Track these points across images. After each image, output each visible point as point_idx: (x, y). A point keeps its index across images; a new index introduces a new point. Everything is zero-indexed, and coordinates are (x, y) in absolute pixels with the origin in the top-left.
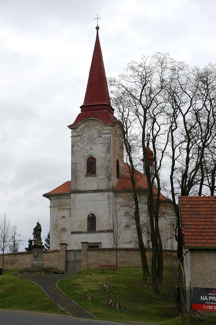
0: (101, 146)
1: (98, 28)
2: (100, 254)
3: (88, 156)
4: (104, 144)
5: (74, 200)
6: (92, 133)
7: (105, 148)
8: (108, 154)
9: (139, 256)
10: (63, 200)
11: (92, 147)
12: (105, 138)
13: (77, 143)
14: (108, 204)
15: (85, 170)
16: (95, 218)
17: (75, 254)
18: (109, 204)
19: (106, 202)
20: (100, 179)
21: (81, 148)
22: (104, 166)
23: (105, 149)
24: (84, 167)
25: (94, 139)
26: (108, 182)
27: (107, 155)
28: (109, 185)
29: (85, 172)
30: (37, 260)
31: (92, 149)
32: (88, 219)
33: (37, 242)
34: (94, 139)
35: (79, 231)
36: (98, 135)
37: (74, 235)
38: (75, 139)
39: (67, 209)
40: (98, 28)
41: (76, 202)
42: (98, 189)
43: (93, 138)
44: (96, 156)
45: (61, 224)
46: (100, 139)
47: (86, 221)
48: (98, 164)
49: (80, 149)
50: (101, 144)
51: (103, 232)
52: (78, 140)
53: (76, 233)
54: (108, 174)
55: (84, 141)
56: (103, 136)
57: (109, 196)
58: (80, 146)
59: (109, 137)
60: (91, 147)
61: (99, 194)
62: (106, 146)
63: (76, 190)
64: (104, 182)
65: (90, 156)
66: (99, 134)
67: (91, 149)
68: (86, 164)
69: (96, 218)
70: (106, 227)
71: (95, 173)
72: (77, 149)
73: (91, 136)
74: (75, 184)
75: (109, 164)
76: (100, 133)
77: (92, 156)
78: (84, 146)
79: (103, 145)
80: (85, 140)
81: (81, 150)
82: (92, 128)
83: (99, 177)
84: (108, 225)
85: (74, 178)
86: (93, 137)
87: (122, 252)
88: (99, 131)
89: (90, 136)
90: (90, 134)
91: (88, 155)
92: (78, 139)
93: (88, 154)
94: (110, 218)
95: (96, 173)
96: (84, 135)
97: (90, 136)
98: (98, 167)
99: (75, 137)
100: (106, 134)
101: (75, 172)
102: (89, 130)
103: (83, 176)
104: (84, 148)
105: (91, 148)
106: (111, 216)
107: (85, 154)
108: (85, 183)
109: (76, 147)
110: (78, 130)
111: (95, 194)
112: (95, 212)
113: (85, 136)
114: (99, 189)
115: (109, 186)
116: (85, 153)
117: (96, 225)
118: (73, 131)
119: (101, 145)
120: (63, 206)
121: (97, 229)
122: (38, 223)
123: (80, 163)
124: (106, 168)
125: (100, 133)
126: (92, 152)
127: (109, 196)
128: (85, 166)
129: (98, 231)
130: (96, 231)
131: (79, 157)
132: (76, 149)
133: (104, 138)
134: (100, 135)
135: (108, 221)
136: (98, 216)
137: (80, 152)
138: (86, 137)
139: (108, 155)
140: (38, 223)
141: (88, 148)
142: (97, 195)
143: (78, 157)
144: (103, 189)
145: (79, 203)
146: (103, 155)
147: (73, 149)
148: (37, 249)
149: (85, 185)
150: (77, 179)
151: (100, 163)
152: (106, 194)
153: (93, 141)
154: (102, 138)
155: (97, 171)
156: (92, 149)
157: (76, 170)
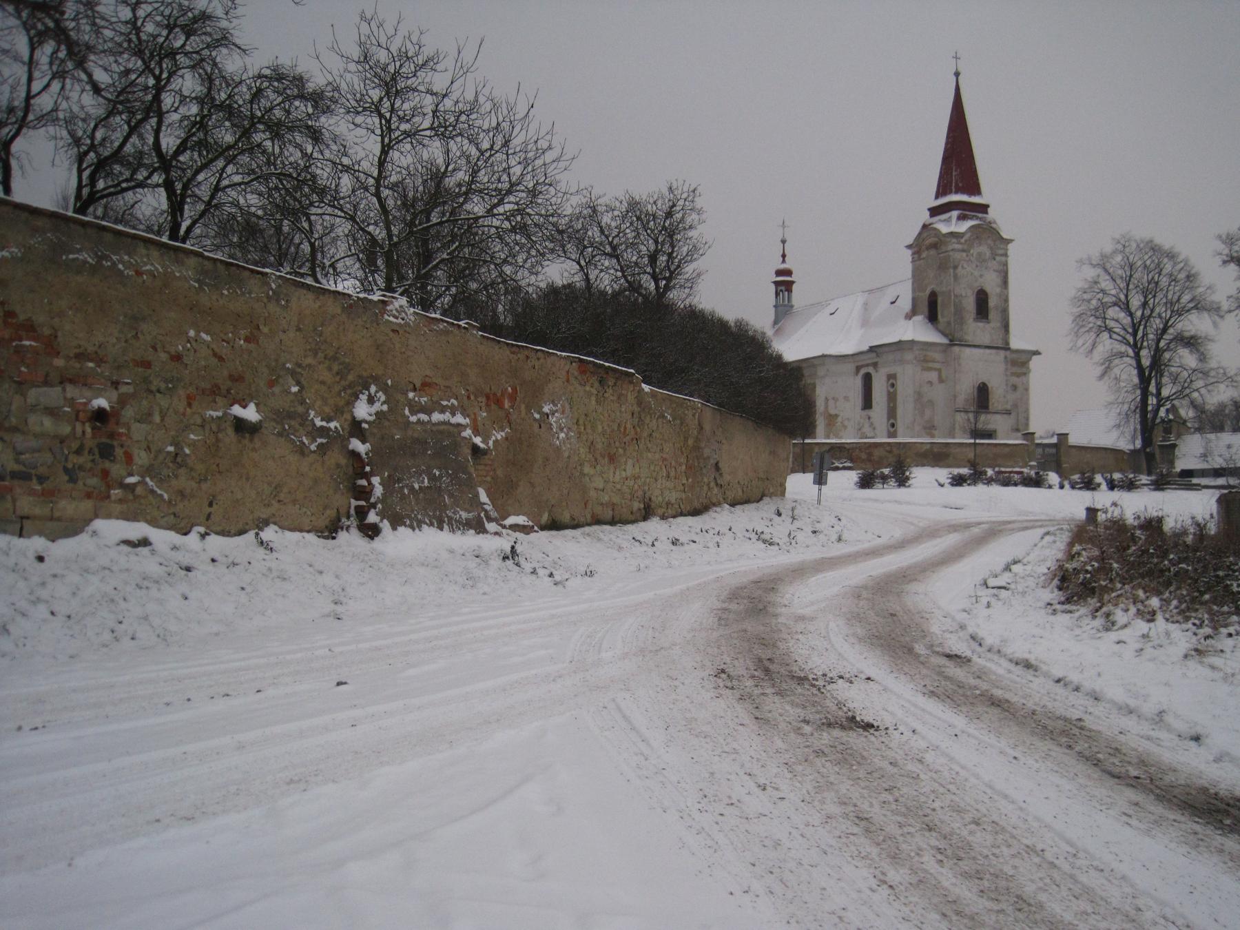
1: (957, 74)
25: (984, 261)
34: (984, 261)
39: (935, 369)
40: (957, 74)
44: (988, 289)
56: (998, 258)
61: (993, 351)
83: (992, 325)
88: (991, 249)
96: (972, 251)
97: (979, 254)
103: (972, 320)
104: (972, 274)
110: (963, 240)
111: (988, 351)
131: (965, 288)
135: (1005, 397)
136: (992, 388)
141: (976, 273)
142: (991, 354)
152: (1002, 353)
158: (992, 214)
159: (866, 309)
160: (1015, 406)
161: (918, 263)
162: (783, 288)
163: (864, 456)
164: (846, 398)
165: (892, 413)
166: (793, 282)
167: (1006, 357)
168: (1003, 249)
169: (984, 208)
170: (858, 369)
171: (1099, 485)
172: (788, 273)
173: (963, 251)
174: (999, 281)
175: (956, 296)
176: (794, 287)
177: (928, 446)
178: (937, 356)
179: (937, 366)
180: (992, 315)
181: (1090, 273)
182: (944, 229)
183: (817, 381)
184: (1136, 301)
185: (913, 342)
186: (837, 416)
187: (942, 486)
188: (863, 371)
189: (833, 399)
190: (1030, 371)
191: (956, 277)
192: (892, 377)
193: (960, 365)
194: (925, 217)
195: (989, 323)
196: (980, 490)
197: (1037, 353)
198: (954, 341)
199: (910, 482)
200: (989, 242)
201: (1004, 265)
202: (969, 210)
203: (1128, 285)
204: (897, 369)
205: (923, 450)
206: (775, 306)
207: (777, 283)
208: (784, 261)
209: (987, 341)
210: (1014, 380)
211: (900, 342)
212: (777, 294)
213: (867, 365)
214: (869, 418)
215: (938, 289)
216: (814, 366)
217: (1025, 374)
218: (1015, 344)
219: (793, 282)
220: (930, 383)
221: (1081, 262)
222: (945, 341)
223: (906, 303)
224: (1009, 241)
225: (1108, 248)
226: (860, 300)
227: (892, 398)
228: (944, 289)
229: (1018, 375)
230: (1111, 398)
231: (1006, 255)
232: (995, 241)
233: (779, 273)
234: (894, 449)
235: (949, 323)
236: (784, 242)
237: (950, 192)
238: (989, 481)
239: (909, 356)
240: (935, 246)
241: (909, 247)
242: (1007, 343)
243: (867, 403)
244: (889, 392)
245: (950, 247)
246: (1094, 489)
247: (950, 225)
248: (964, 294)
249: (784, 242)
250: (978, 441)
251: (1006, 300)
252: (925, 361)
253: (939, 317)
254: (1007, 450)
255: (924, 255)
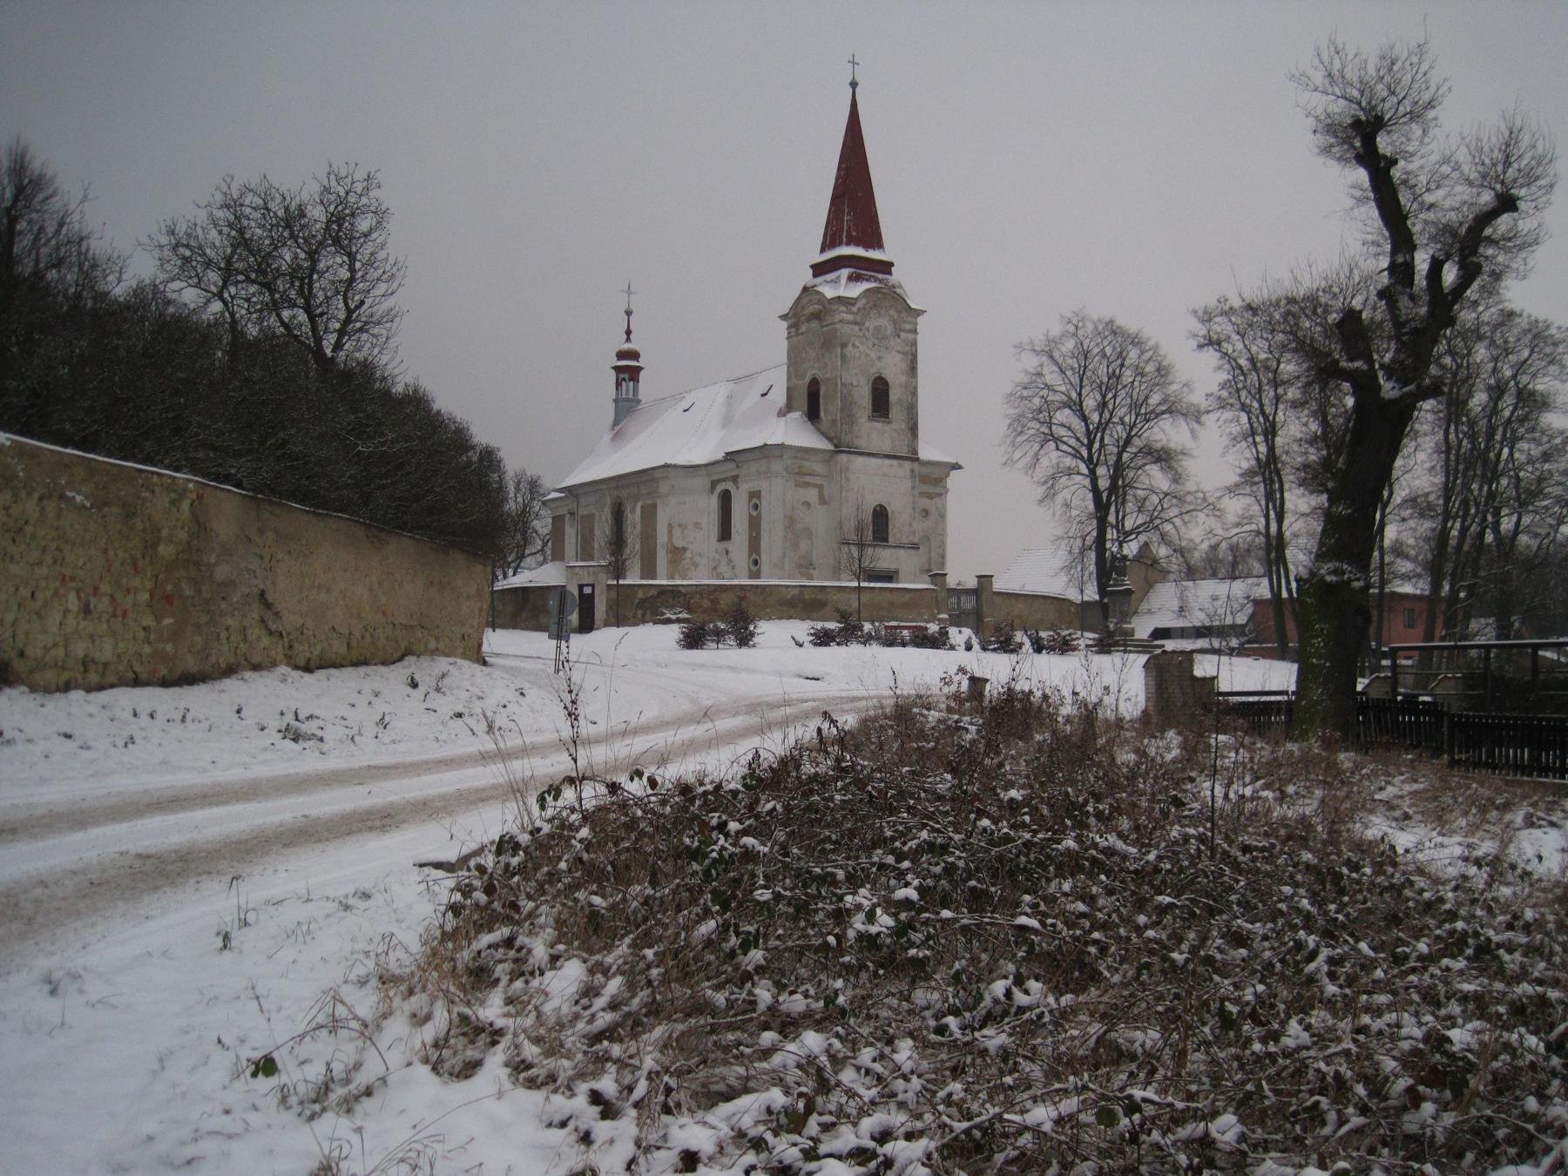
0: (898, 358)
1: (854, 85)
19: (908, 484)
25: (885, 338)
34: (885, 338)
39: (815, 485)
40: (854, 85)
46: (898, 340)
56: (903, 335)
61: (895, 462)
83: (894, 426)
88: (895, 322)
93: (874, 370)
96: (867, 324)
97: (877, 329)
103: (865, 419)
104: (867, 355)
108: (869, 435)
109: (850, 347)
110: (855, 309)
111: (887, 462)
121: (891, 539)
152: (907, 464)
158: (897, 275)
159: (729, 405)
160: (926, 538)
161: (795, 339)
162: (626, 376)
163: (706, 604)
164: (697, 525)
165: (754, 545)
166: (639, 369)
167: (913, 471)
168: (910, 323)
169: (886, 267)
170: (714, 484)
171: (1021, 645)
172: (634, 355)
173: (855, 323)
174: (904, 366)
175: (843, 385)
176: (642, 374)
177: (796, 591)
178: (819, 468)
179: (817, 480)
180: (895, 412)
181: (1031, 362)
182: (829, 292)
183: (658, 501)
184: (1090, 403)
185: (782, 446)
186: (685, 549)
187: (801, 646)
188: (720, 488)
189: (680, 525)
190: (947, 491)
191: (844, 359)
192: (755, 495)
193: (848, 480)
194: (807, 277)
196: (855, 649)
197: (957, 467)
198: (841, 447)
199: (756, 639)
200: (892, 312)
202: (862, 268)
203: (1081, 380)
204: (762, 485)
205: (789, 596)
206: (616, 401)
207: (618, 369)
208: (628, 340)
209: (886, 447)
210: (925, 502)
211: (765, 445)
212: (618, 384)
213: (725, 480)
214: (727, 552)
215: (820, 375)
216: (655, 480)
217: (940, 495)
218: (926, 452)
219: (639, 369)
220: (807, 504)
221: (1020, 348)
222: (830, 447)
223: (779, 396)
224: (919, 313)
225: (1056, 331)
226: (722, 391)
227: (755, 523)
228: (828, 375)
229: (930, 496)
230: (1059, 531)
231: (915, 331)
232: (899, 312)
233: (621, 355)
234: (750, 596)
235: (834, 422)
236: (629, 313)
237: (840, 244)
238: (867, 640)
239: (777, 466)
240: (817, 316)
241: (784, 317)
242: (916, 452)
243: (725, 533)
244: (751, 516)
245: (837, 318)
246: (1012, 651)
247: (838, 287)
248: (855, 383)
249: (629, 313)
250: (863, 584)
251: (914, 393)
252: (800, 473)
253: (822, 414)
254: (908, 597)
255: (803, 329)
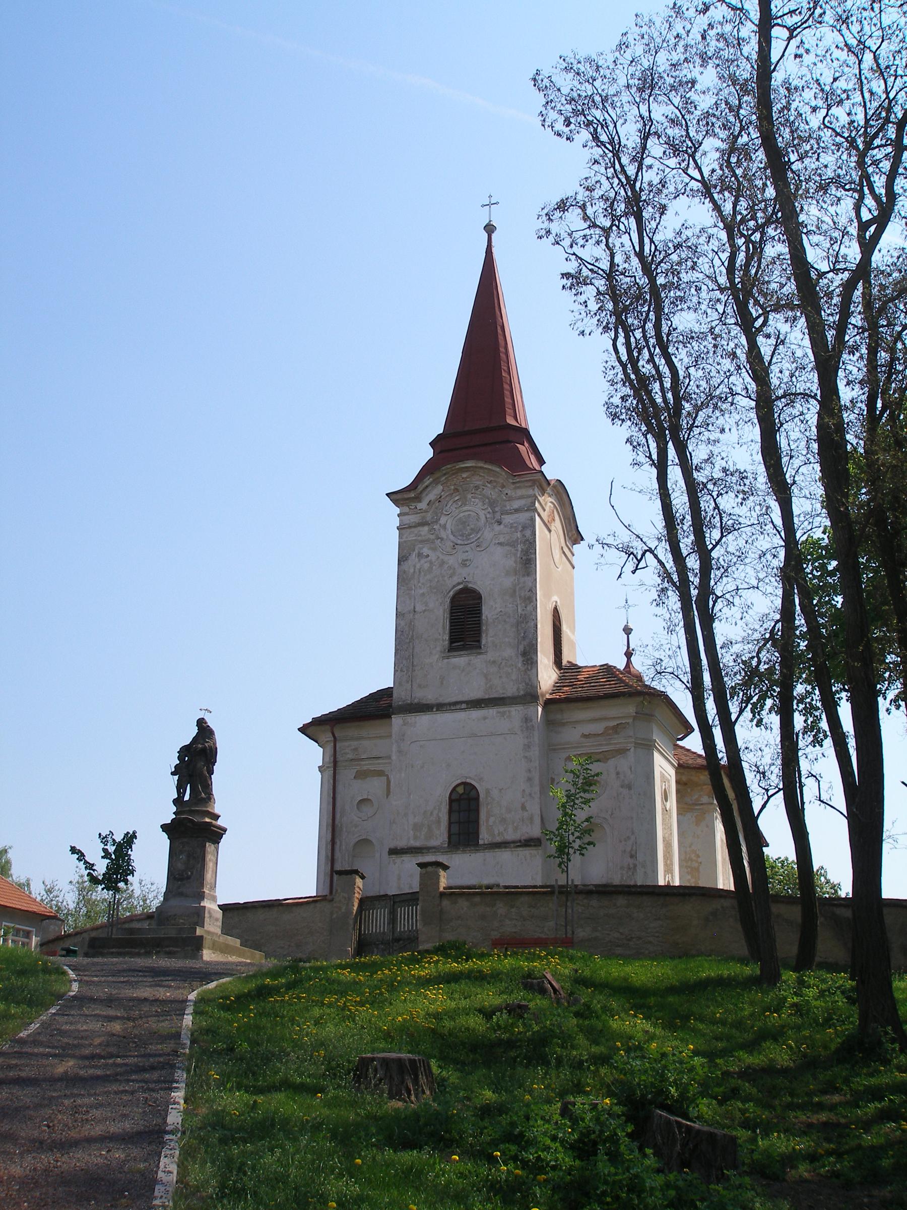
1: (490, 229)
2: (494, 909)
3: (454, 586)
4: (512, 544)
5: (403, 735)
6: (469, 513)
7: (513, 559)
8: (524, 576)
9: (656, 919)
10: (365, 743)
11: (469, 558)
12: (515, 525)
13: (417, 548)
14: (525, 745)
15: (441, 633)
16: (477, 798)
17: (393, 913)
18: (529, 747)
20: (494, 662)
21: (431, 562)
22: (509, 617)
23: (515, 562)
24: (441, 624)
25: (476, 530)
26: (523, 669)
27: (522, 580)
28: (527, 681)
29: (443, 640)
30: (181, 894)
31: (468, 563)
32: (451, 801)
33: (188, 809)
34: (476, 530)
35: (417, 844)
36: (488, 516)
37: (398, 860)
38: (411, 536)
40: (490, 229)
41: (409, 743)
42: (487, 697)
43: (472, 529)
44: (481, 585)
45: (356, 826)
46: (497, 528)
47: (445, 809)
48: (489, 612)
49: (427, 566)
50: (500, 544)
51: (506, 847)
52: (419, 538)
53: (406, 853)
54: (525, 643)
55: (442, 539)
56: (508, 519)
57: (526, 719)
58: (428, 556)
59: (528, 522)
60: (465, 556)
61: (491, 712)
62: (517, 550)
63: (409, 702)
64: (510, 671)
65: (461, 587)
66: (494, 512)
67: (464, 564)
68: (447, 615)
69: (481, 799)
70: (516, 829)
71: (479, 641)
72: (418, 566)
73: (465, 522)
74: (408, 682)
75: (528, 608)
76: (497, 509)
77: (470, 585)
78: (440, 555)
79: (508, 548)
80: (445, 537)
81: (430, 570)
82: (469, 496)
83: (491, 655)
84: (523, 820)
85: (404, 662)
86: (472, 526)
87: (585, 901)
88: (492, 504)
89: (463, 523)
90: (462, 515)
91: (454, 583)
92: (420, 535)
93: (456, 579)
94: (530, 794)
95: (483, 642)
96: (443, 520)
97: (463, 523)
98: (490, 620)
99: (413, 530)
100: (517, 511)
101: (409, 642)
102: (460, 503)
104: (443, 563)
105: (467, 560)
106: (537, 789)
107: (445, 581)
108: (442, 679)
110: (423, 505)
112: (476, 775)
113: (445, 525)
114: (492, 696)
115: (527, 684)
116: (446, 578)
117: (481, 822)
118: (406, 509)
119: (499, 548)
120: (364, 763)
121: (485, 837)
122: (201, 723)
123: (425, 610)
124: (518, 624)
125: (497, 509)
126: (469, 575)
127: (527, 720)
128: (442, 621)
129: (490, 844)
130: (481, 842)
131: (423, 594)
132: (415, 566)
133: (512, 524)
134: (498, 516)
135: (523, 808)
136: (488, 792)
137: (428, 577)
138: (448, 526)
139: (526, 578)
140: (201, 723)
141: (451, 561)
142: (485, 718)
143: (421, 592)
144: (505, 696)
145: (421, 746)
146: (508, 582)
147: (405, 566)
148: (185, 840)
149: (442, 683)
150: (415, 663)
151: (496, 608)
152: (516, 712)
153: (473, 538)
154: (502, 526)
155: (484, 635)
156: (468, 563)
157: (412, 636)
195: (480, 653)
201: (524, 528)
